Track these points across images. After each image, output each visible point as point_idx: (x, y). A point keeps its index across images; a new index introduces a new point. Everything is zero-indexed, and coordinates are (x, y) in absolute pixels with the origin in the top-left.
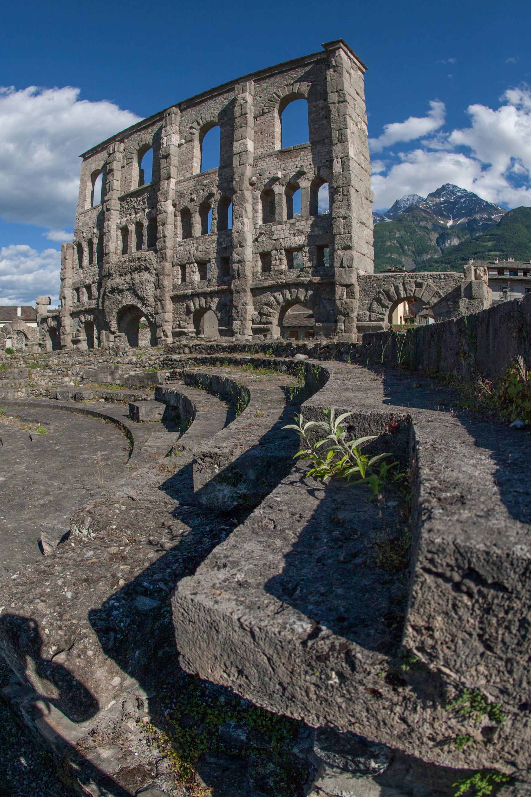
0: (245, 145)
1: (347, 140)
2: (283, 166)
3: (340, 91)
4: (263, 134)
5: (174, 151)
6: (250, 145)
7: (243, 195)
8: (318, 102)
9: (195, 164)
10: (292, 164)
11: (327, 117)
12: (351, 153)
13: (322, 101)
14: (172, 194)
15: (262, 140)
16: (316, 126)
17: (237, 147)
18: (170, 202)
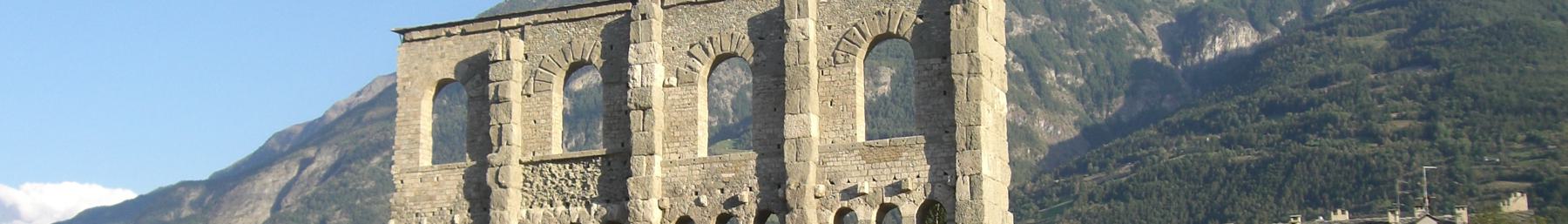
0: (806, 125)
1: (979, 147)
2: (872, 172)
3: (971, 53)
4: (835, 104)
5: (657, 98)
6: (814, 121)
7: (803, 215)
8: (932, 61)
9: (700, 133)
10: (887, 171)
11: (949, 90)
12: (985, 171)
13: (939, 60)
14: (657, 187)
15: (834, 116)
16: (929, 107)
17: (792, 126)
18: (654, 202)
